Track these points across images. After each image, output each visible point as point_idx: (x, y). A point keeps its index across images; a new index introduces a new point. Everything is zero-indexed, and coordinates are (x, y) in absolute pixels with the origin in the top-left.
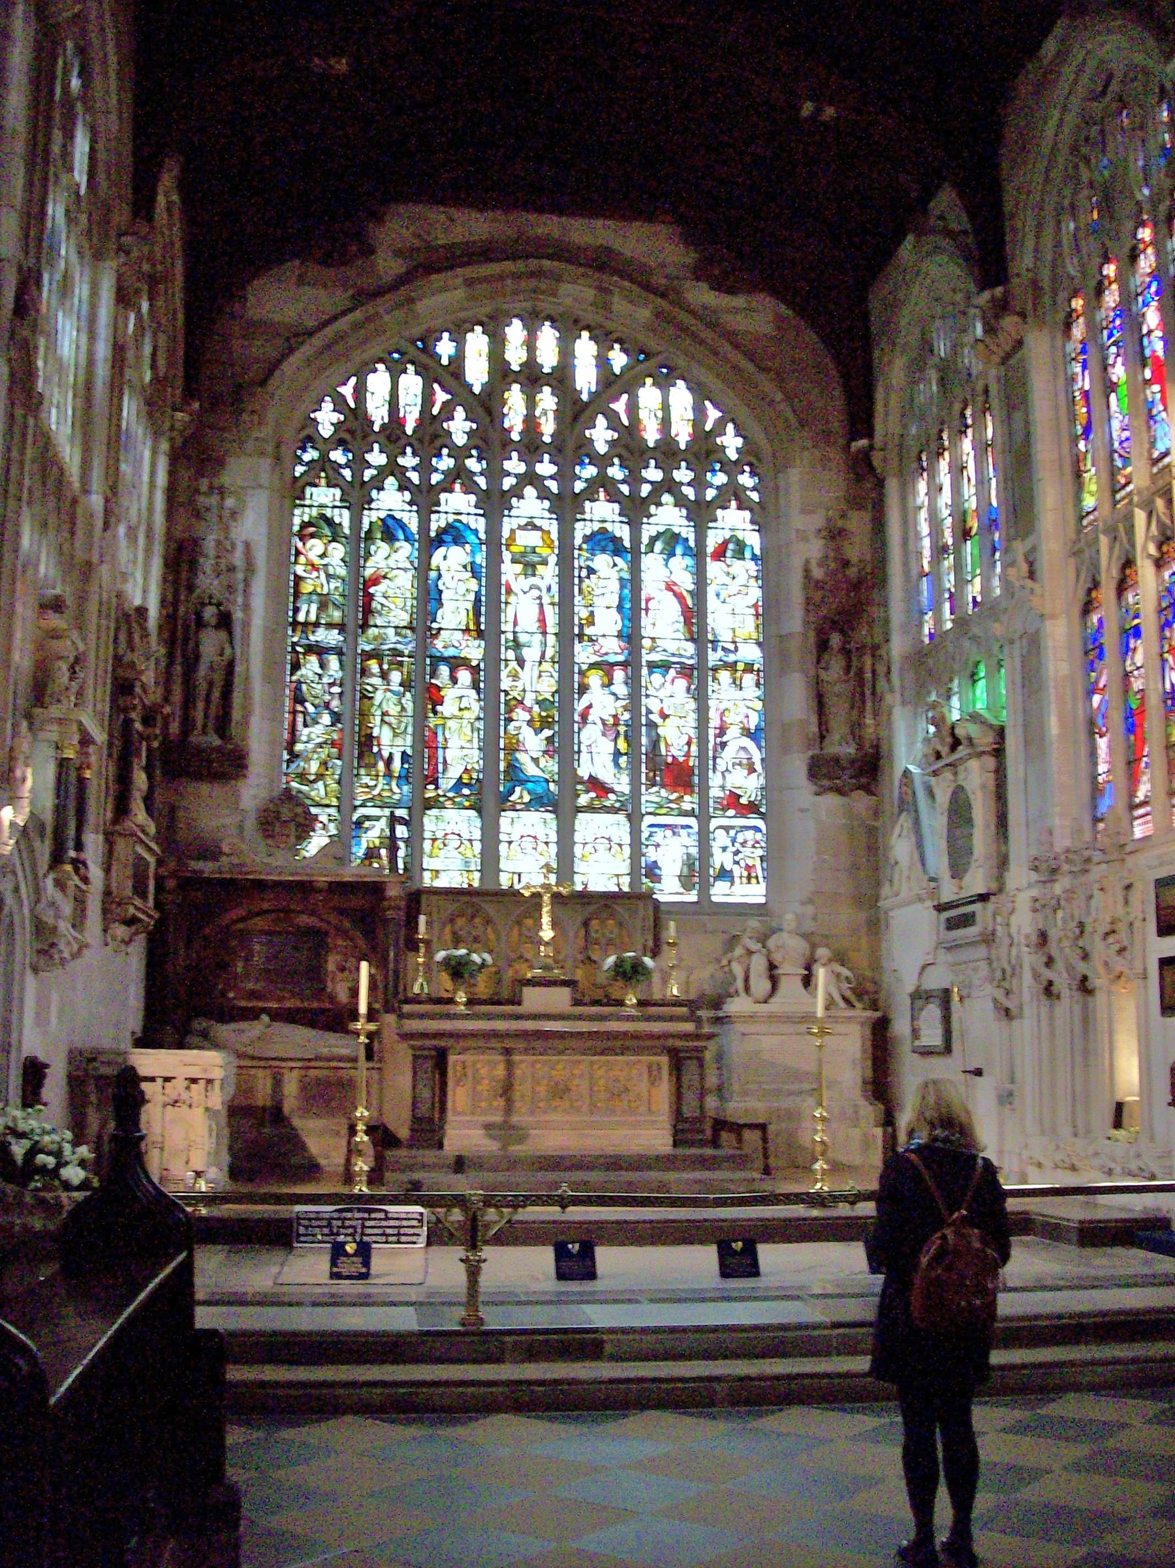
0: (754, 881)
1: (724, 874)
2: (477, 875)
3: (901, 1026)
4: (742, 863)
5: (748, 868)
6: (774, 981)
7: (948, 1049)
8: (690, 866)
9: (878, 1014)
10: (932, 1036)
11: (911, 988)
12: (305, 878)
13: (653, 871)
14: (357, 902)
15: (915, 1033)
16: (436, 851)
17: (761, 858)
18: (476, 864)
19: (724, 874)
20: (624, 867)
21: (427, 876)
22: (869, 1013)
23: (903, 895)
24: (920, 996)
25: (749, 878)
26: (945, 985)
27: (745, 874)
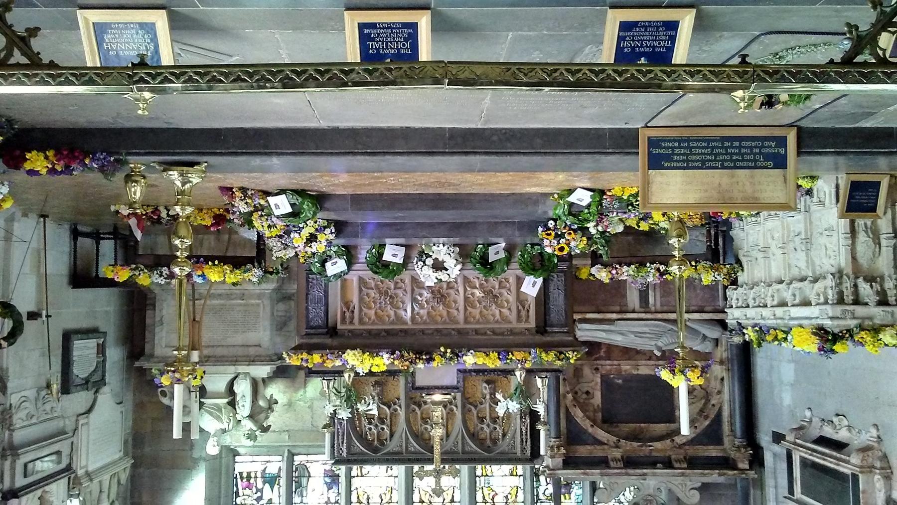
0: (245, 475)
1: (271, 481)
2: (479, 473)
3: (115, 354)
4: (254, 490)
5: (249, 487)
6: (231, 391)
7: (68, 337)
8: (299, 485)
9: (137, 364)
10: (84, 352)
11: (105, 389)
12: (631, 471)
13: (333, 479)
14: (583, 451)
15: (101, 350)
16: (514, 492)
17: (238, 495)
18: (480, 482)
19: (271, 481)
20: (356, 482)
21: (520, 472)
22: (146, 365)
23: (106, 478)
24: (94, 383)
25: (249, 477)
26: (65, 397)
27: (252, 481)
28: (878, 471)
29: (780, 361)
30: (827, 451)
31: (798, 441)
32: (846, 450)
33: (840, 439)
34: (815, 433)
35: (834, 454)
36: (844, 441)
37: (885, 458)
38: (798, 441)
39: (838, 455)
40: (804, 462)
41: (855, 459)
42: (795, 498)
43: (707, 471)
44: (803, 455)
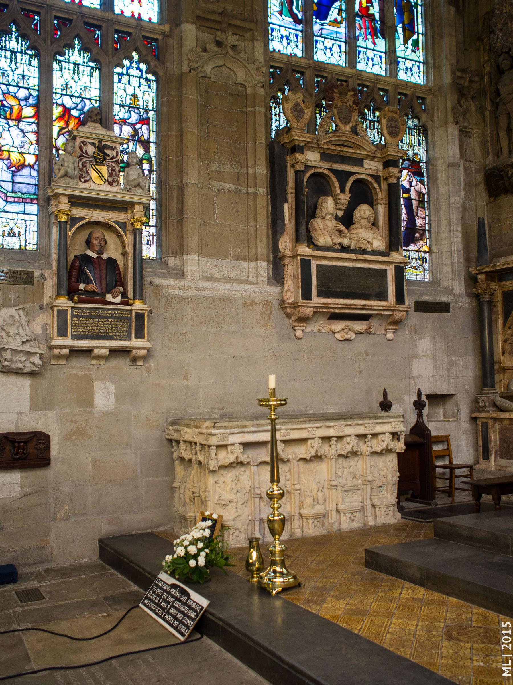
28: (286, 305)
29: (434, 376)
30: (347, 311)
31: (390, 313)
32: (328, 316)
33: (341, 322)
34: (374, 323)
35: (336, 311)
36: (336, 322)
37: (289, 316)
38: (390, 313)
39: (332, 310)
40: (382, 296)
41: (309, 311)
42: (394, 265)
43: (505, 267)
44: (384, 303)
